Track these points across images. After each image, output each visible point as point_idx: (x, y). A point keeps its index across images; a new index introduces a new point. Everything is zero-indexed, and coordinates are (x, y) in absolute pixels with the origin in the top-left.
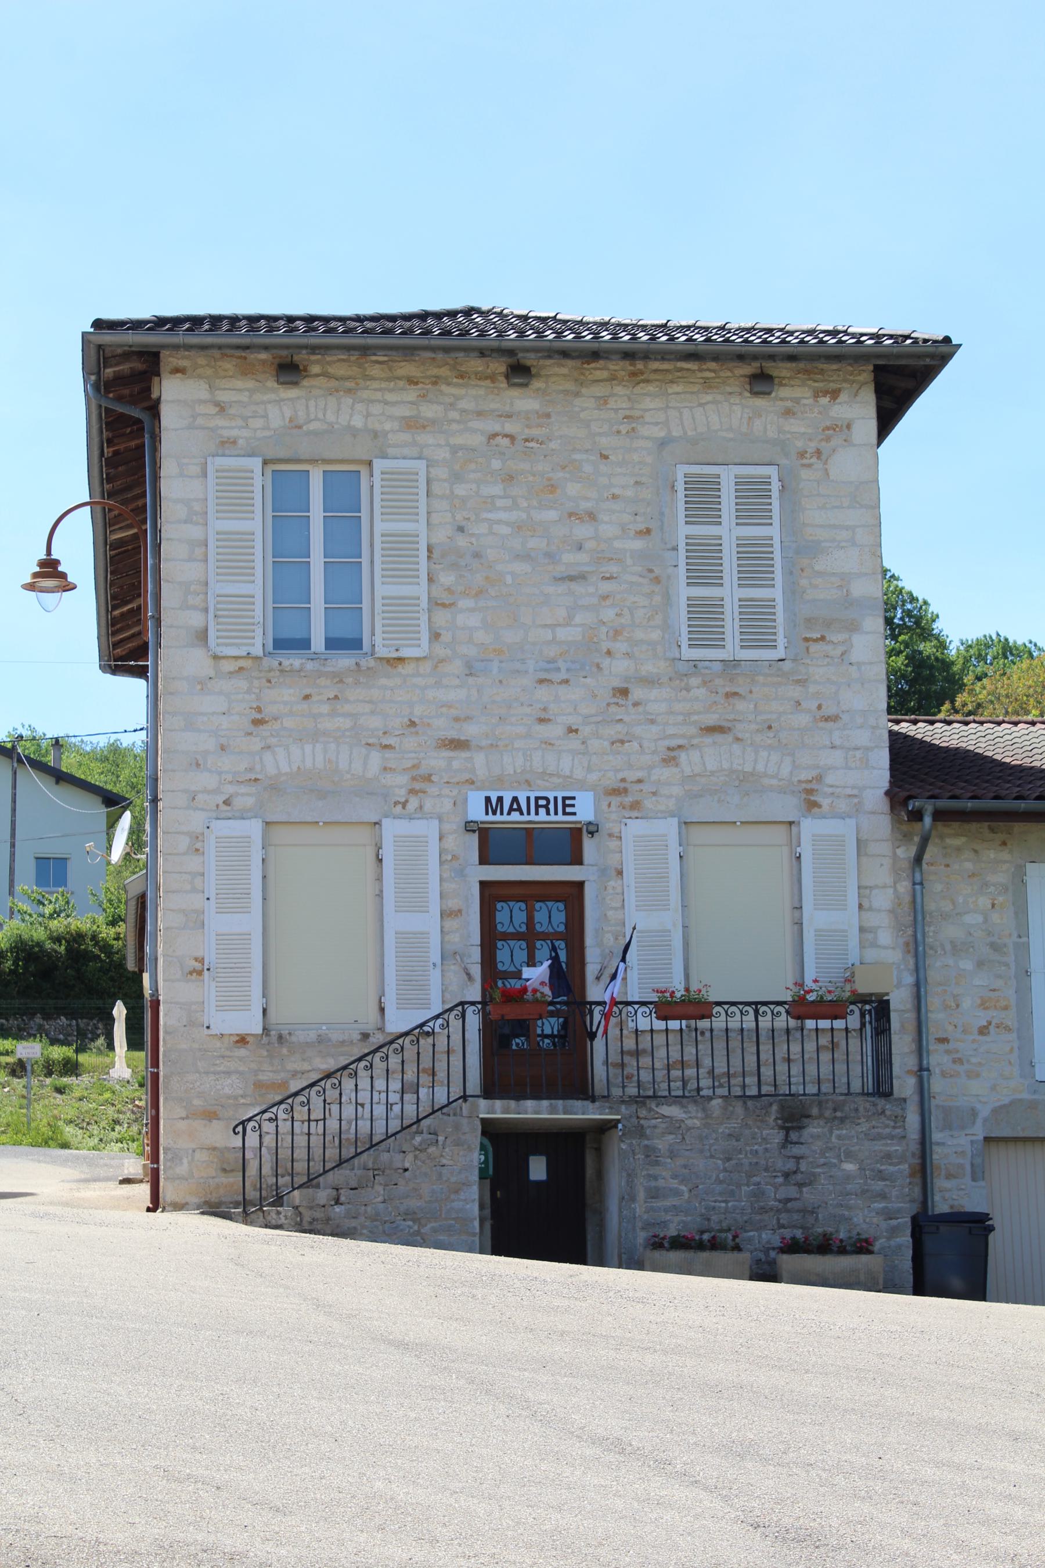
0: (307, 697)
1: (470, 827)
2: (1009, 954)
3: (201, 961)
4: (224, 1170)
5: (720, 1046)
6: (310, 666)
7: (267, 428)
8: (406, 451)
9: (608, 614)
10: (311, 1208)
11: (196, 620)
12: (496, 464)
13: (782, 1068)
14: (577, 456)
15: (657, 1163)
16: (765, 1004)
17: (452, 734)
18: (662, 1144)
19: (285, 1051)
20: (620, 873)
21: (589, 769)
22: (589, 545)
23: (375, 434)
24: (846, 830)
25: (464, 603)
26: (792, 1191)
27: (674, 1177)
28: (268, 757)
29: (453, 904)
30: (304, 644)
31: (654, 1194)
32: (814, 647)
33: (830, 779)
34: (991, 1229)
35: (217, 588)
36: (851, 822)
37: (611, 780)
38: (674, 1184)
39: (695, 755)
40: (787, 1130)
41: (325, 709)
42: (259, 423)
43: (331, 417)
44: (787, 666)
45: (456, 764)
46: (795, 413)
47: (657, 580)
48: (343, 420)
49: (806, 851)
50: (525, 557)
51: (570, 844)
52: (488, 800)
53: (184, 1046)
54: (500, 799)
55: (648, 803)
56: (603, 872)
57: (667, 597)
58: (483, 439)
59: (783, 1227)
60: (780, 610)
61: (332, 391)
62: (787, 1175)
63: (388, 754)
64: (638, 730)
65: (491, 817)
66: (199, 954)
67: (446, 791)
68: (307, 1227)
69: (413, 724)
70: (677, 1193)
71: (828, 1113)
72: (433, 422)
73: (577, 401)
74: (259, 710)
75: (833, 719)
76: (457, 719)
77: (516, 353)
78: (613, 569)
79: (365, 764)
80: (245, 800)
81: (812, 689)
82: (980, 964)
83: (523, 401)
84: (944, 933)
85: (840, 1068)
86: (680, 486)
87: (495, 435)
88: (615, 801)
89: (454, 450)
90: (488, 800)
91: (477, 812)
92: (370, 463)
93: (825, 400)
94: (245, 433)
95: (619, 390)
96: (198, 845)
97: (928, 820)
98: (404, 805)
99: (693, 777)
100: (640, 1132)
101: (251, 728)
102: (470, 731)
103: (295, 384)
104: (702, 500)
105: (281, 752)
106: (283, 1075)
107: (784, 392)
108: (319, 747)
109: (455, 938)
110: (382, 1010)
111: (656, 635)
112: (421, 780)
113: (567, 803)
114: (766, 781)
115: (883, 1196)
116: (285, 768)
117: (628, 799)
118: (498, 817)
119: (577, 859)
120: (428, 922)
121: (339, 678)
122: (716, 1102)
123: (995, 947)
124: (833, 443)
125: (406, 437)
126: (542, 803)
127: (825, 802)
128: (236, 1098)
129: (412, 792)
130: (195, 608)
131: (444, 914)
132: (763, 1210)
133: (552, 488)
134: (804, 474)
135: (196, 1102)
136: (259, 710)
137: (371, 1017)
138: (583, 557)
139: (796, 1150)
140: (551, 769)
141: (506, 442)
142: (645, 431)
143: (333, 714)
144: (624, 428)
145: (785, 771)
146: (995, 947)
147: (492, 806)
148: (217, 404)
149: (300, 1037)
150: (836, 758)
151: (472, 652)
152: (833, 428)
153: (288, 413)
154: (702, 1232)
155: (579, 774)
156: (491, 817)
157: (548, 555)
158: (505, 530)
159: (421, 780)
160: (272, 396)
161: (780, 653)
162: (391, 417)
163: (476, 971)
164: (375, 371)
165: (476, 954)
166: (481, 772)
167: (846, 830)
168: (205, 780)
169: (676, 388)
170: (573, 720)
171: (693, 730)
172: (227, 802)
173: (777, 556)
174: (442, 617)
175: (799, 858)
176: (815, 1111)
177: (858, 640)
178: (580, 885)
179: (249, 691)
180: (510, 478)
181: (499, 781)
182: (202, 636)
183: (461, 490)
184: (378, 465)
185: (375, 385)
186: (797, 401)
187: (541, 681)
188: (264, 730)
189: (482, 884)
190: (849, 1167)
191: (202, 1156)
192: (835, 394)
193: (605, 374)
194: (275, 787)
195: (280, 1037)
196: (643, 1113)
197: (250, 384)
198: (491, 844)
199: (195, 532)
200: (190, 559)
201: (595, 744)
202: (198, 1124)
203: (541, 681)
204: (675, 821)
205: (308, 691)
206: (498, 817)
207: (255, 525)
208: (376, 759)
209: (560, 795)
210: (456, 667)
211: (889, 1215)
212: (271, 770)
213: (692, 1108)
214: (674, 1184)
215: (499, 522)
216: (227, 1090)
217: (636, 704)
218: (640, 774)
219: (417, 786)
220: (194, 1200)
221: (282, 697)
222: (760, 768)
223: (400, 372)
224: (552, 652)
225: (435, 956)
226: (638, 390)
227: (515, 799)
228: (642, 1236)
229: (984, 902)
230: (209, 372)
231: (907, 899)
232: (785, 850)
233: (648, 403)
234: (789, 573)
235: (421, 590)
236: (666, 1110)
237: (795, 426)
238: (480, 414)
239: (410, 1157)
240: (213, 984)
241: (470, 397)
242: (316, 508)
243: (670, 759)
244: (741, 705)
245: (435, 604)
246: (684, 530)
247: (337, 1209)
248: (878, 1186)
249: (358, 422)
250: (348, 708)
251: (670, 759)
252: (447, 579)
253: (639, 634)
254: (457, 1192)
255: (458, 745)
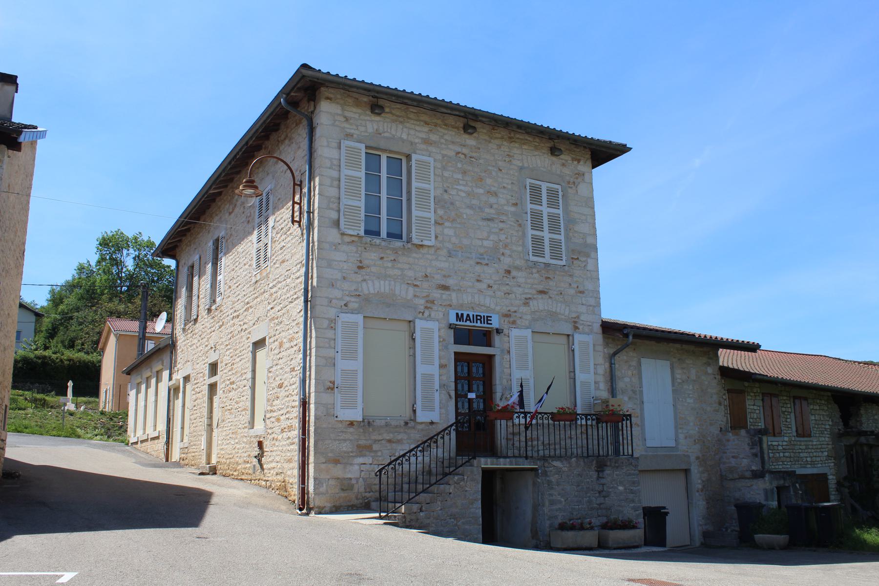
0: (382, 258)
1: (451, 326)
2: (637, 394)
3: (333, 383)
4: (343, 490)
5: (546, 431)
6: (383, 244)
7: (366, 131)
8: (424, 153)
9: (503, 237)
10: (410, 514)
11: (334, 215)
12: (459, 165)
13: (568, 441)
14: (490, 168)
15: (552, 488)
16: (590, 415)
17: (443, 283)
18: (554, 479)
19: (371, 430)
20: (509, 352)
21: (497, 305)
22: (495, 206)
23: (412, 143)
24: (589, 339)
25: (447, 224)
26: (601, 500)
27: (559, 494)
28: (364, 284)
29: (444, 362)
30: (378, 234)
31: (552, 503)
32: (575, 262)
33: (582, 318)
34: (667, 514)
35: (344, 201)
36: (591, 336)
37: (505, 310)
38: (559, 498)
39: (535, 302)
40: (598, 472)
41: (390, 265)
42: (363, 129)
43: (393, 132)
44: (566, 268)
45: (444, 297)
46: (564, 166)
47: (520, 225)
48: (398, 134)
49: (576, 347)
50: (471, 207)
51: (486, 337)
52: (457, 314)
53: (324, 426)
54: (462, 314)
55: (518, 322)
56: (502, 351)
57: (524, 235)
58: (454, 153)
59: (599, 516)
60: (563, 244)
61: (393, 121)
62: (599, 492)
63: (417, 289)
64: (515, 289)
65: (458, 323)
66: (332, 379)
67: (440, 309)
68: (408, 524)
69: (427, 276)
70: (560, 502)
71: (613, 464)
72: (435, 142)
73: (490, 145)
74: (361, 262)
75: (582, 292)
76: (445, 276)
77: (470, 120)
78: (504, 218)
79: (407, 292)
80: (354, 305)
81: (575, 279)
82: (630, 398)
83: (470, 141)
84: (620, 385)
85: (585, 441)
86: (528, 188)
87: (458, 153)
88: (507, 319)
89: (444, 156)
90: (457, 314)
91: (453, 320)
92: (409, 157)
93: (576, 163)
94: (357, 132)
95: (505, 143)
96: (332, 325)
97: (631, 337)
98: (423, 313)
99: (534, 312)
100: (545, 473)
101: (357, 270)
102: (450, 282)
103: (379, 114)
104: (536, 193)
105: (370, 282)
106: (370, 442)
107: (562, 156)
108: (387, 282)
109: (444, 378)
110: (414, 411)
111: (520, 249)
112: (430, 303)
113: (488, 319)
114: (560, 316)
115: (633, 501)
116: (372, 291)
117: (512, 319)
118: (461, 323)
119: (489, 344)
120: (434, 370)
121: (395, 251)
122: (574, 459)
123: (634, 392)
124: (579, 180)
125: (423, 146)
126: (478, 318)
127: (581, 327)
128: (348, 453)
129: (426, 307)
130: (332, 209)
131: (442, 366)
132: (592, 509)
133: (481, 179)
134: (570, 190)
135: (330, 455)
136: (361, 262)
137: (408, 413)
138: (492, 211)
139: (603, 481)
140: (482, 303)
141: (462, 156)
142: (514, 162)
143: (393, 267)
144: (507, 159)
145: (567, 313)
146: (634, 392)
147: (459, 317)
148: (345, 117)
149: (378, 423)
150: (583, 309)
151: (450, 246)
152: (578, 174)
153: (375, 127)
154: (570, 520)
155: (493, 306)
156: (458, 323)
157: (480, 208)
158: (463, 195)
159: (430, 303)
160: (368, 118)
161: (563, 263)
162: (417, 137)
163: (453, 394)
164: (412, 116)
165: (453, 385)
166: (454, 302)
167: (589, 339)
168: (337, 293)
169: (525, 147)
170: (491, 282)
171: (535, 292)
172: (346, 305)
173: (562, 222)
174: (439, 228)
175: (573, 351)
176: (608, 464)
177: (589, 260)
178: (491, 357)
179: (356, 252)
180: (465, 173)
181: (461, 306)
182: (337, 223)
183: (446, 174)
184: (414, 157)
185: (412, 122)
186: (567, 161)
187: (478, 263)
188: (363, 272)
189: (456, 353)
190: (621, 488)
191: (332, 482)
192: (579, 161)
193: (500, 136)
194: (366, 300)
195: (369, 423)
196: (546, 464)
197: (359, 111)
198: (462, 335)
199: (335, 174)
200: (331, 186)
201: (499, 294)
202: (330, 466)
203: (478, 263)
204: (530, 330)
205: (382, 255)
206: (461, 323)
207: (362, 174)
208: (411, 290)
209: (486, 315)
210: (444, 252)
211: (635, 509)
212: (366, 292)
213: (565, 462)
214: (559, 498)
215: (461, 190)
216: (344, 449)
217: (513, 278)
218: (515, 309)
219: (429, 305)
220: (328, 505)
221: (371, 257)
222: (558, 311)
223: (422, 118)
224: (482, 251)
225: (437, 386)
226: (512, 145)
227: (468, 315)
228: (548, 523)
229: (630, 373)
230: (342, 102)
231: (608, 370)
232: (566, 346)
233: (516, 151)
234: (566, 230)
235: (432, 215)
236: (557, 464)
237: (566, 171)
238: (453, 142)
239: (452, 487)
240: (339, 395)
241: (450, 135)
242: (388, 170)
243: (526, 304)
244: (551, 283)
245: (437, 223)
246: (529, 206)
247: (422, 514)
248: (631, 496)
249: (404, 136)
250: (399, 265)
251: (526, 304)
252: (441, 212)
253: (514, 248)
254: (472, 504)
255: (445, 288)
